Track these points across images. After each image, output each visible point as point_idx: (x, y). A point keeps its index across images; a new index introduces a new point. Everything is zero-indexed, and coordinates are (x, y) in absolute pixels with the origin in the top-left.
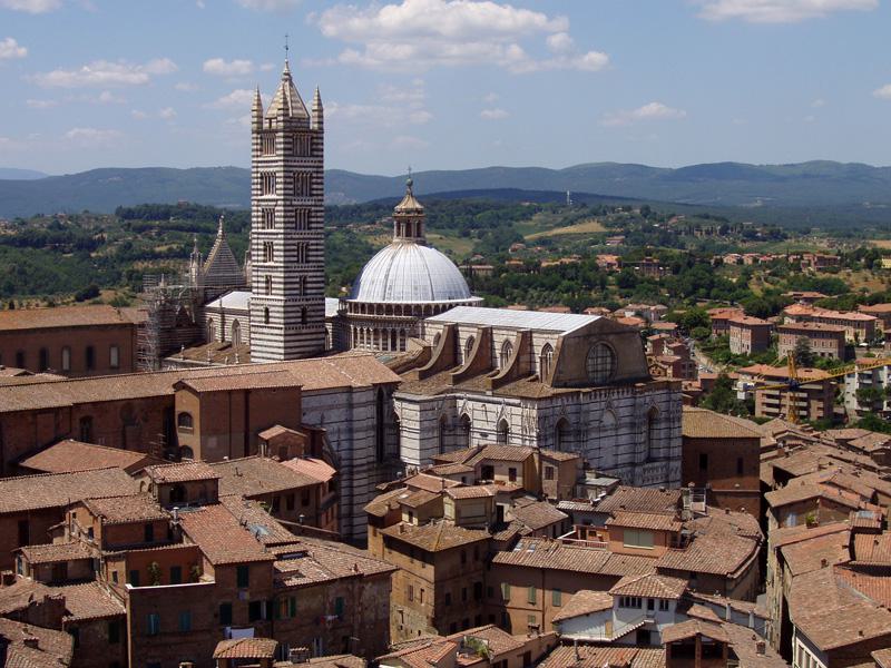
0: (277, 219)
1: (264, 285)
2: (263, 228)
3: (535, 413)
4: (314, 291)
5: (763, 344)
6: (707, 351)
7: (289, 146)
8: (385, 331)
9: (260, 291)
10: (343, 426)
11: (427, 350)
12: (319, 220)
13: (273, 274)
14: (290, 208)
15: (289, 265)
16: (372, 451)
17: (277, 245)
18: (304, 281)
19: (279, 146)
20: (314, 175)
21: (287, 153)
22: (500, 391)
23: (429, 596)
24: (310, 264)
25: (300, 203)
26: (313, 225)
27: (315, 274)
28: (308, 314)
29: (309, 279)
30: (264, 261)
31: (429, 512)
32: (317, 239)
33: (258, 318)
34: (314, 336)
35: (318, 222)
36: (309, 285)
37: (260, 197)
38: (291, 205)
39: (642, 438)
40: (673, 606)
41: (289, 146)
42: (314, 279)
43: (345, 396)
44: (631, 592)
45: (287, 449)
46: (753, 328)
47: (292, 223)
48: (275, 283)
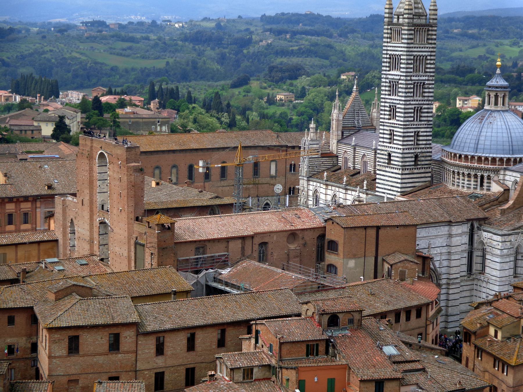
0: (400, 90)
1: (388, 136)
2: (390, 95)
4: (424, 142)
7: (411, 37)
8: (476, 176)
9: (385, 140)
10: (444, 250)
11: (507, 190)
12: (431, 90)
13: (395, 129)
14: (410, 82)
15: (407, 123)
16: (465, 268)
17: (399, 108)
18: (417, 134)
19: (404, 36)
20: (429, 58)
21: (410, 41)
24: (423, 122)
25: (417, 78)
26: (426, 94)
27: (425, 130)
28: (419, 159)
29: (421, 134)
30: (389, 119)
32: (428, 104)
33: (382, 158)
34: (423, 175)
35: (429, 92)
36: (421, 138)
37: (388, 73)
38: (411, 80)
41: (411, 37)
42: (425, 134)
43: (447, 228)
45: (405, 272)
47: (411, 92)
48: (396, 135)
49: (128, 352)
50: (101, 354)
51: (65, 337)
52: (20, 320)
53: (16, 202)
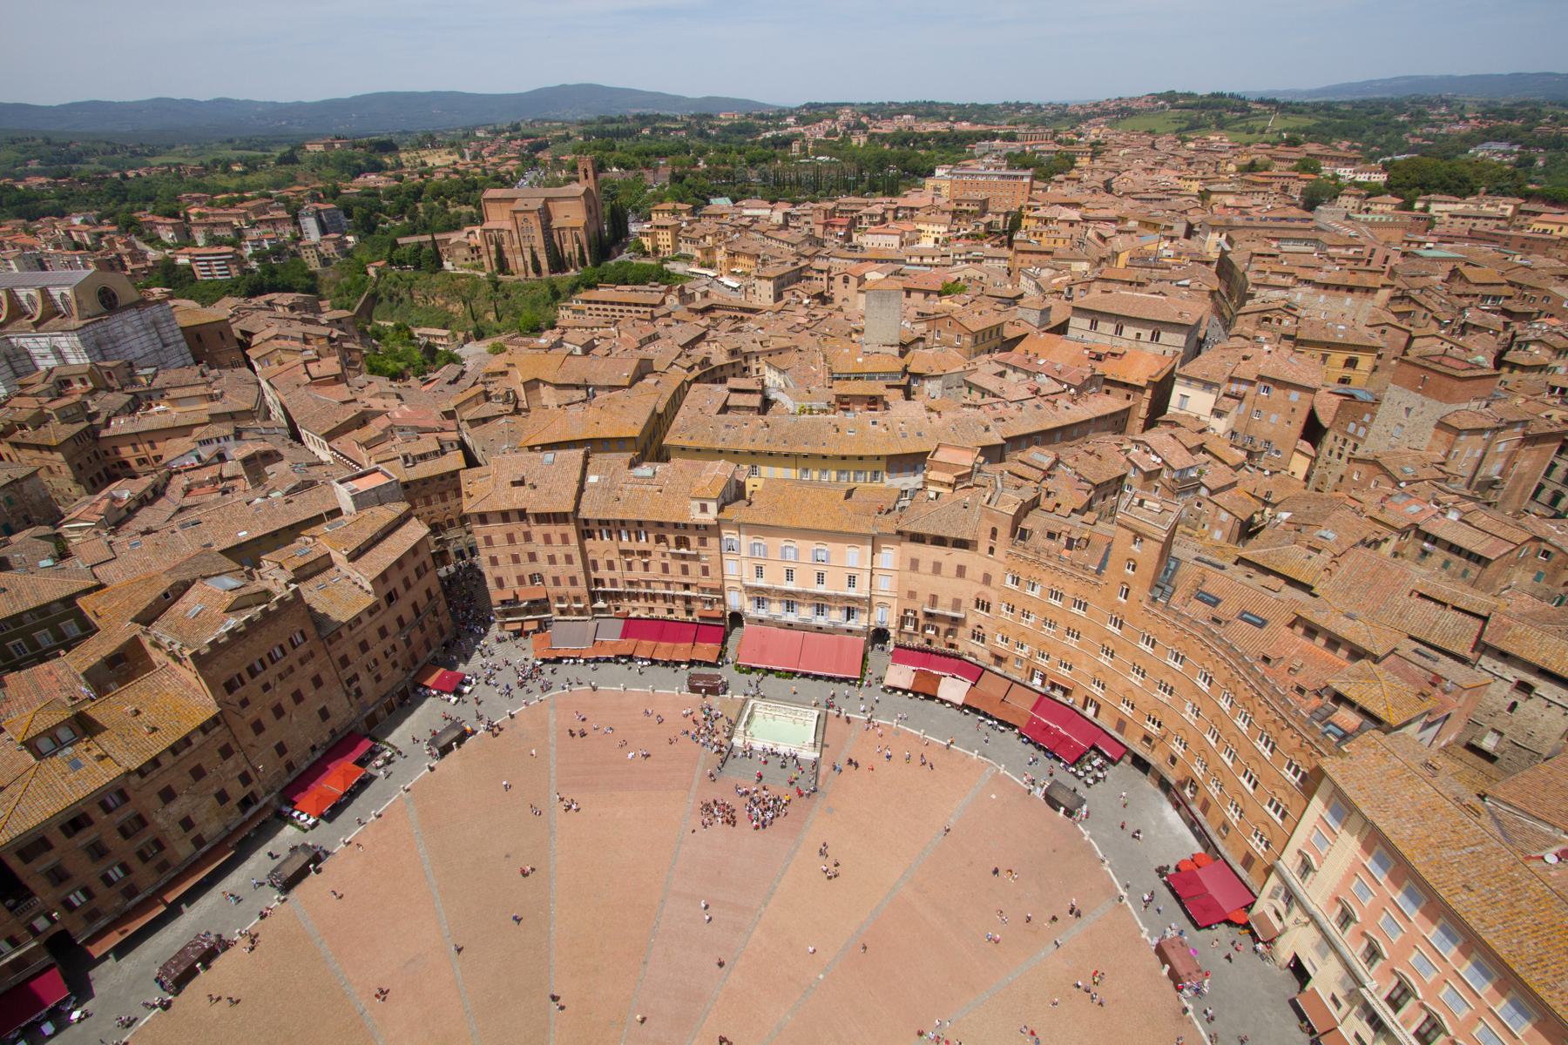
3: (76, 339)
5: (185, 238)
6: (149, 242)
22: (41, 328)
23: (66, 468)
31: (40, 420)
39: (155, 335)
40: (232, 438)
44: (205, 438)
46: (172, 225)
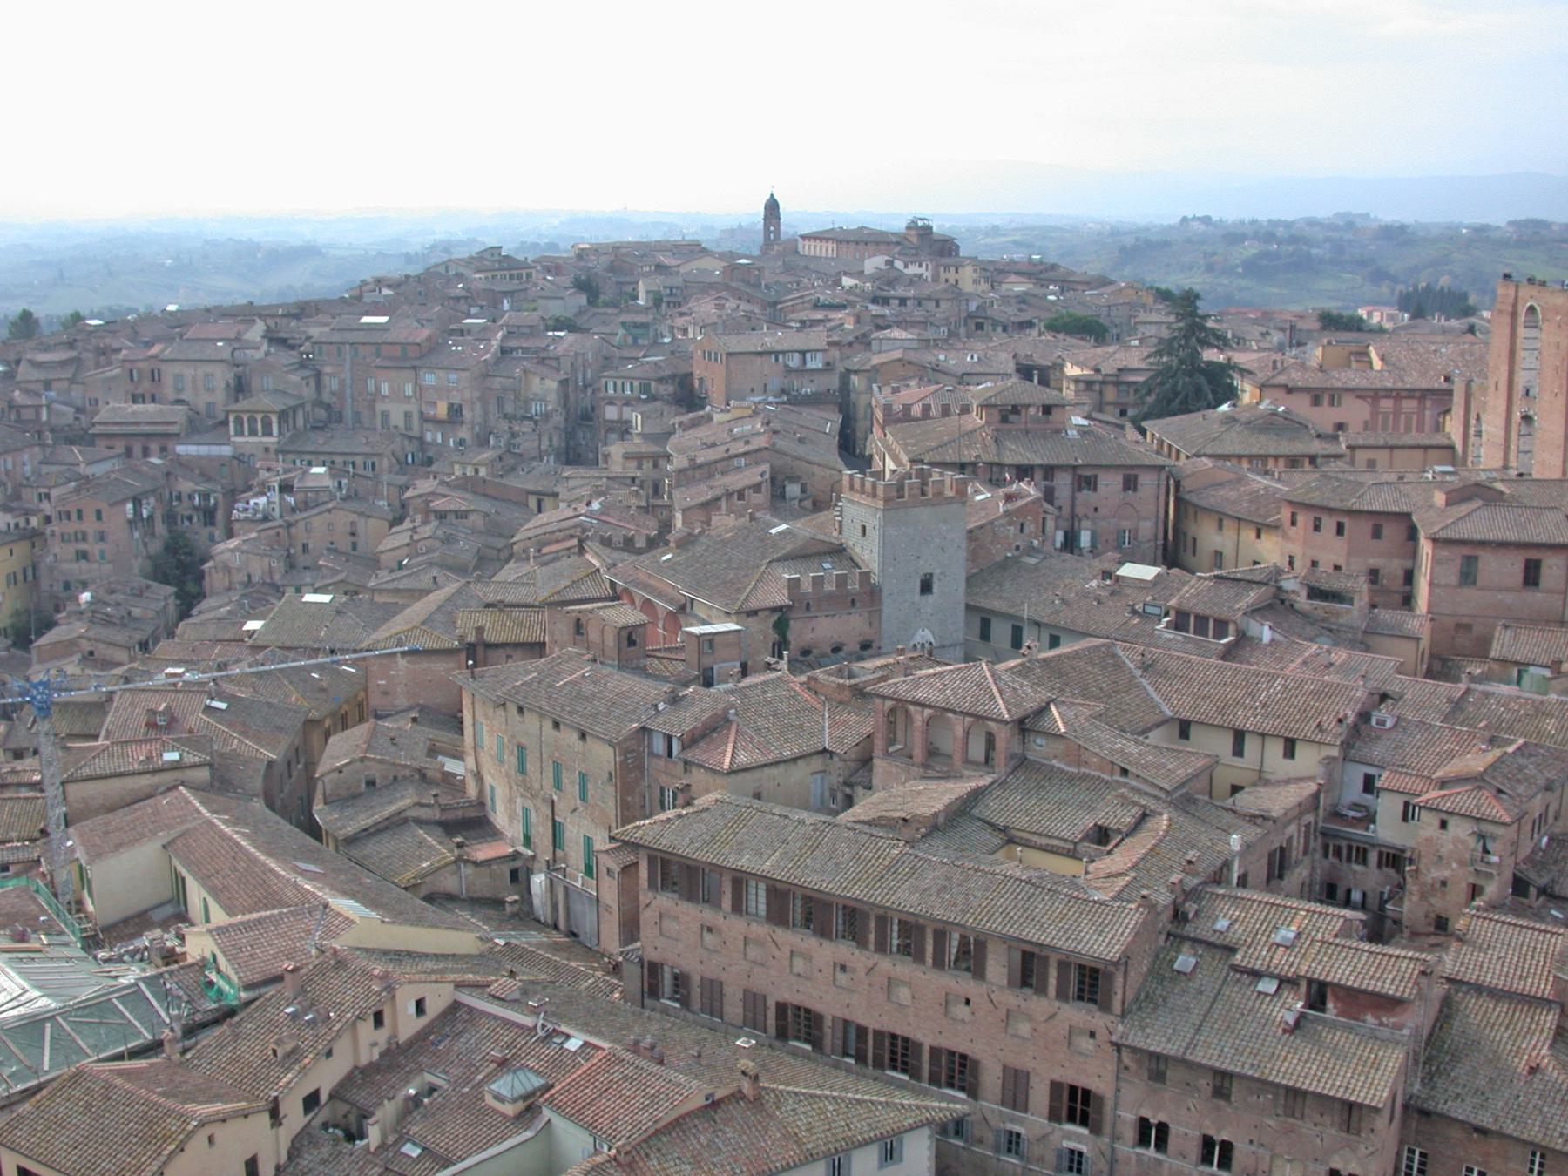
49: (1552, 592)
50: (1508, 590)
51: (1456, 555)
52: (1391, 531)
53: (1395, 398)
